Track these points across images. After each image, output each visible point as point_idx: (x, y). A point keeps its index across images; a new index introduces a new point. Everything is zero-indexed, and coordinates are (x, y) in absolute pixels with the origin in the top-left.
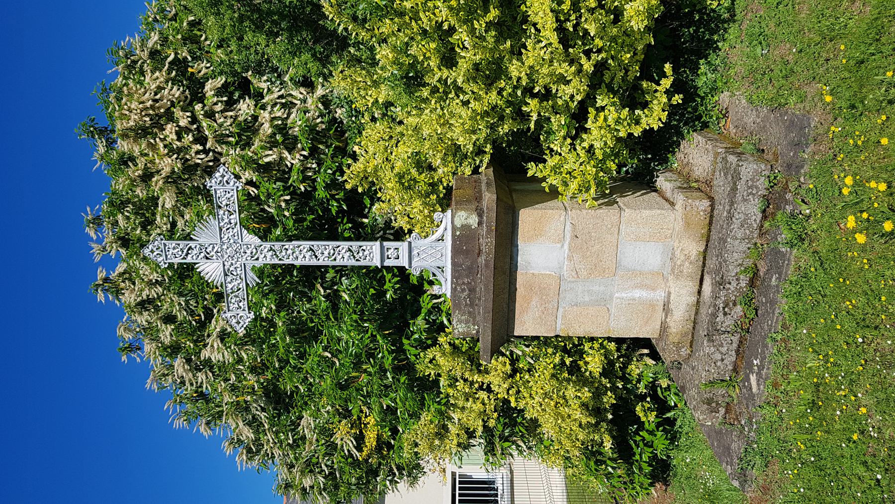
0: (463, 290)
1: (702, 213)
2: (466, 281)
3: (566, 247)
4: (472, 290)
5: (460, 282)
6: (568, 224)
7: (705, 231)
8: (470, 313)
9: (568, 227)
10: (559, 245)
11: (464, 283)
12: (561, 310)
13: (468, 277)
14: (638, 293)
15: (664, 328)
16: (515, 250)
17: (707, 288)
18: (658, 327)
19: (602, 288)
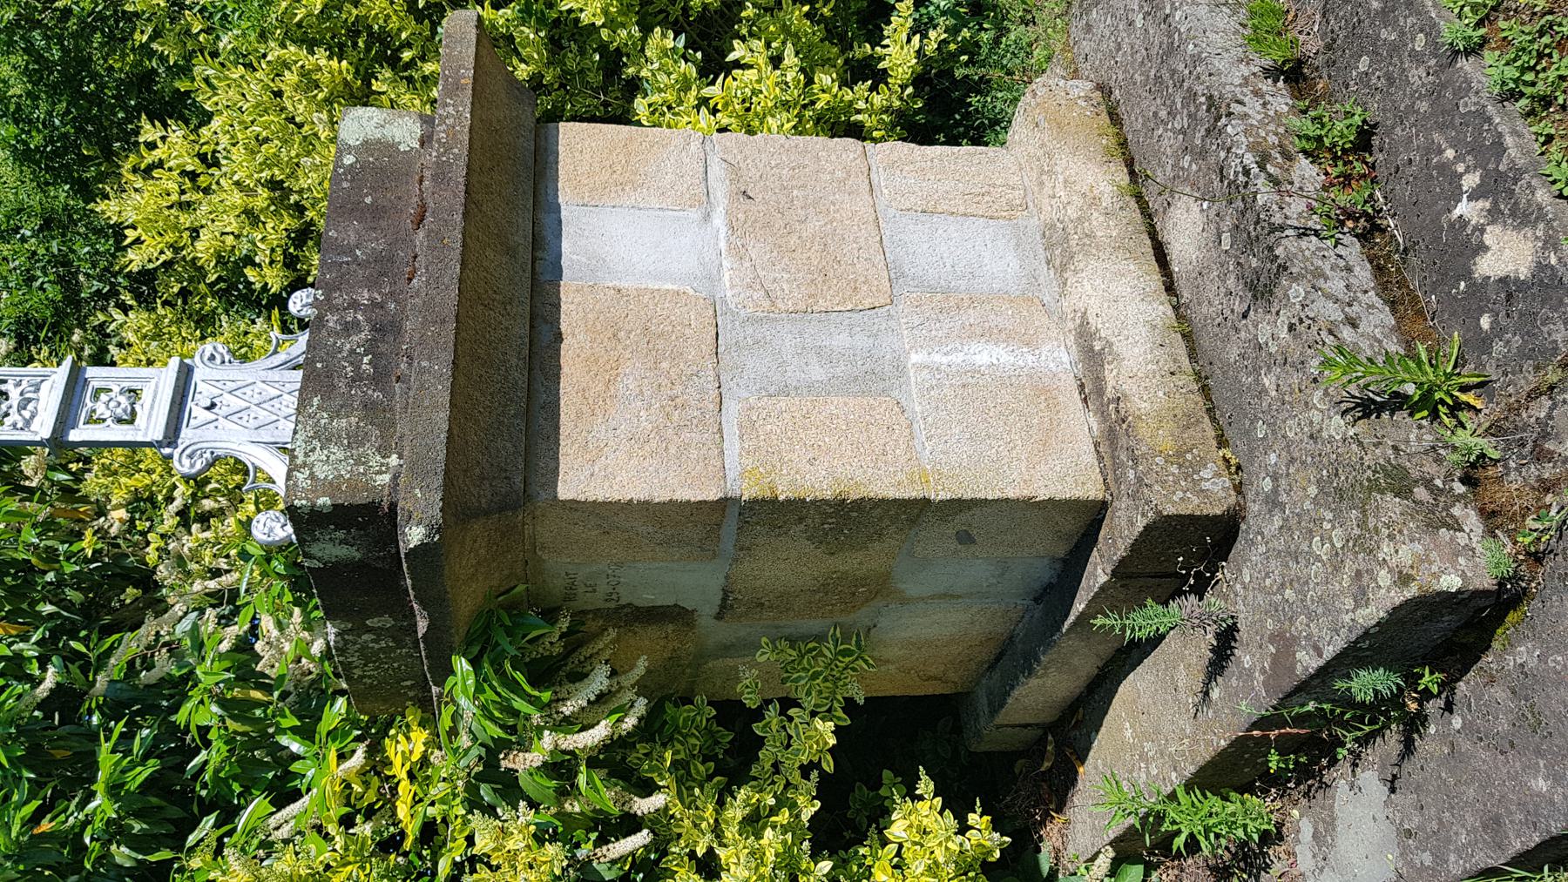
0: (349, 328)
1: (1081, 103)
2: (364, 297)
3: (719, 220)
4: (386, 329)
5: (340, 299)
6: (716, 170)
7: (1109, 141)
8: (369, 407)
9: (716, 170)
10: (695, 214)
11: (354, 305)
12: (732, 408)
13: (372, 284)
14: (984, 355)
15: (1115, 436)
16: (547, 220)
17: (1187, 227)
18: (1091, 458)
19: (862, 341)
